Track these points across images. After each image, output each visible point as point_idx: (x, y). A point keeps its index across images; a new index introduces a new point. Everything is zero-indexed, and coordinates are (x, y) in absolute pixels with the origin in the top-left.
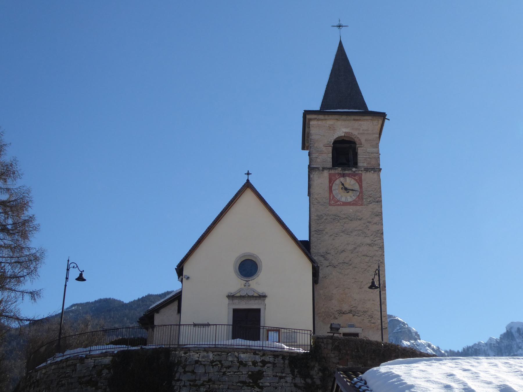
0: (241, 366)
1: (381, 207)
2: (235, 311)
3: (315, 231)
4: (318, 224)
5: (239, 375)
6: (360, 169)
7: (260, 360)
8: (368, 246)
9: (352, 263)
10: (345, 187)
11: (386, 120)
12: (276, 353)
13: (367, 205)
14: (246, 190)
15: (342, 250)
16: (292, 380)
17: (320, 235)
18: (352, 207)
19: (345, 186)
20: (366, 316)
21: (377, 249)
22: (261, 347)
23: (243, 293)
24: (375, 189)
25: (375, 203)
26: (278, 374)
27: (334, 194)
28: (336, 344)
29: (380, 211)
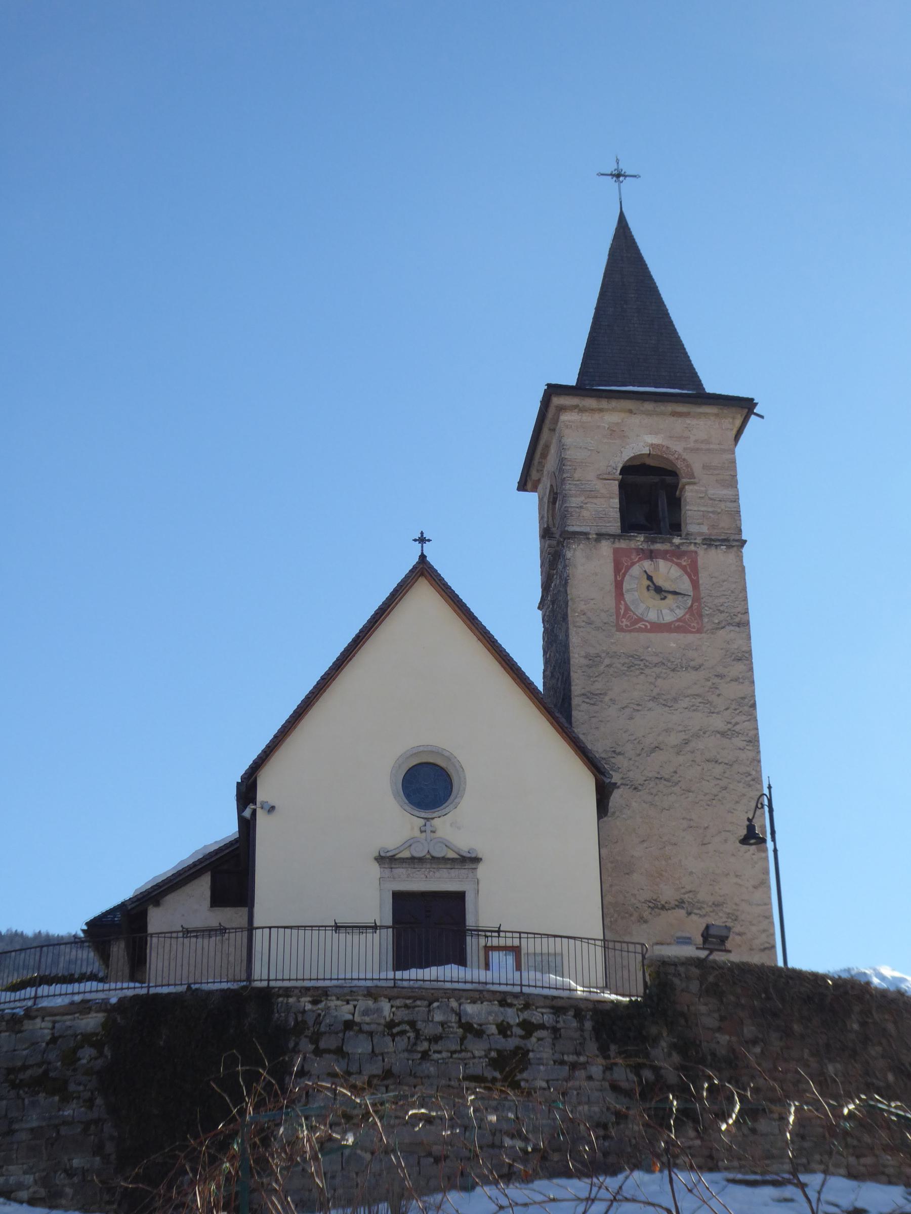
0: (468, 1035)
2: (398, 897)
3: (583, 695)
4: (590, 677)
5: (465, 1059)
7: (517, 1021)
8: (718, 735)
9: (680, 779)
10: (657, 584)
11: (753, 417)
12: (560, 1003)
13: (712, 633)
14: (416, 580)
15: (653, 746)
16: (604, 1072)
17: (595, 707)
18: (674, 635)
20: (721, 914)
23: (419, 852)
24: (732, 592)
25: (732, 628)
26: (566, 1058)
27: (628, 602)
28: (711, 979)
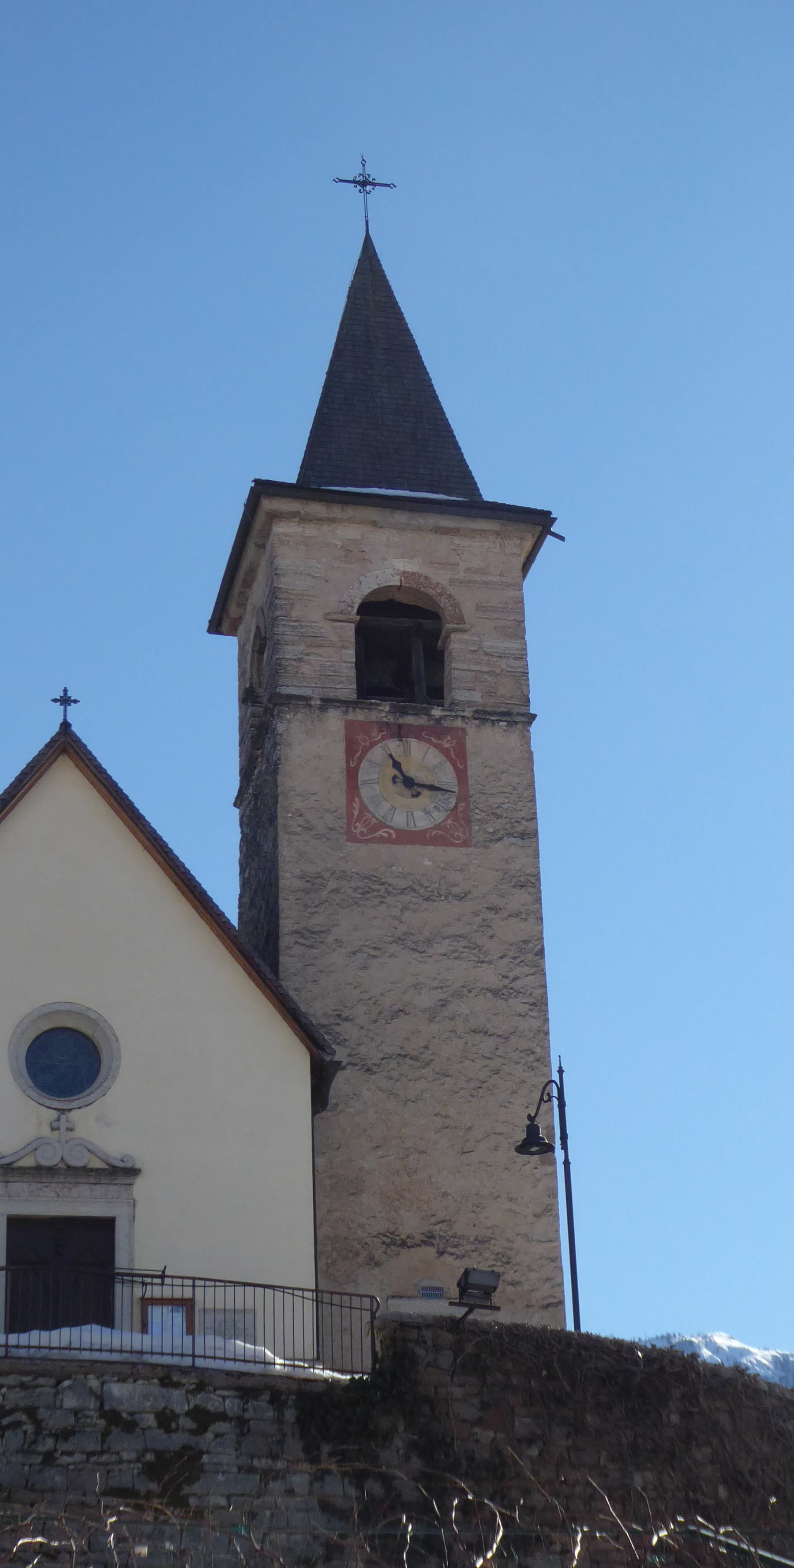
0: (113, 1428)
1: (537, 855)
2: (15, 1224)
3: (296, 932)
4: (306, 906)
5: (108, 1464)
6: (458, 713)
7: (186, 1408)
8: (489, 995)
9: (432, 1057)
10: (407, 774)
11: (549, 538)
12: (249, 1382)
13: (485, 847)
15: (396, 1008)
16: (311, 1484)
17: (315, 951)
18: (431, 848)
19: (404, 770)
20: (486, 1255)
21: (524, 1008)
22: (185, 1358)
23: (48, 1158)
24: (515, 789)
25: (513, 840)
26: (256, 1462)
27: (366, 801)
28: (470, 1348)
29: (530, 870)
